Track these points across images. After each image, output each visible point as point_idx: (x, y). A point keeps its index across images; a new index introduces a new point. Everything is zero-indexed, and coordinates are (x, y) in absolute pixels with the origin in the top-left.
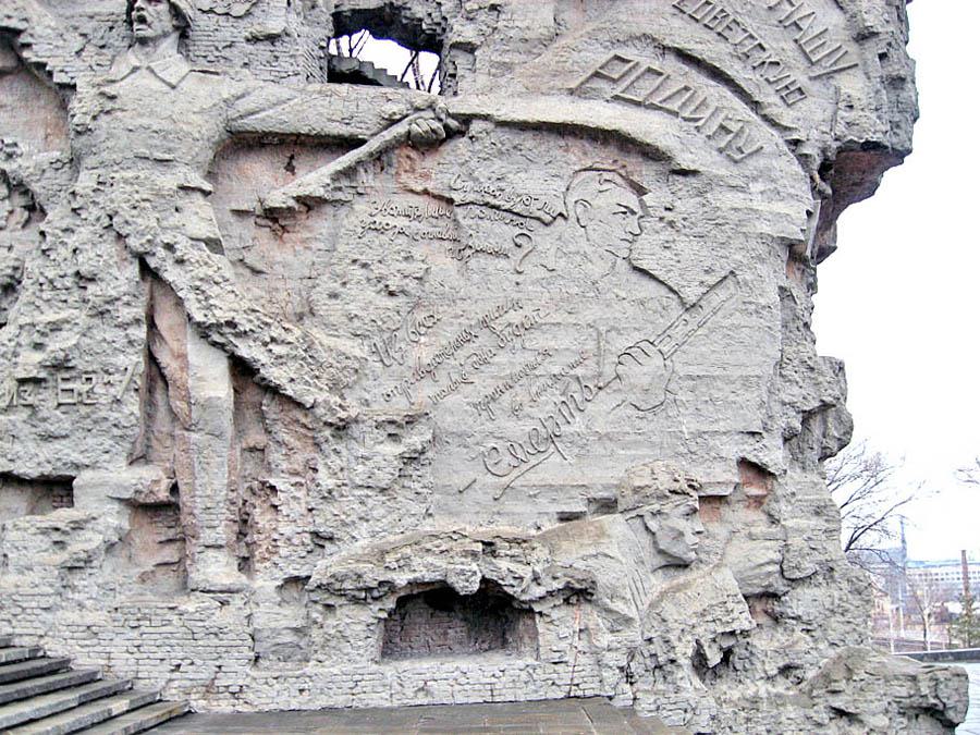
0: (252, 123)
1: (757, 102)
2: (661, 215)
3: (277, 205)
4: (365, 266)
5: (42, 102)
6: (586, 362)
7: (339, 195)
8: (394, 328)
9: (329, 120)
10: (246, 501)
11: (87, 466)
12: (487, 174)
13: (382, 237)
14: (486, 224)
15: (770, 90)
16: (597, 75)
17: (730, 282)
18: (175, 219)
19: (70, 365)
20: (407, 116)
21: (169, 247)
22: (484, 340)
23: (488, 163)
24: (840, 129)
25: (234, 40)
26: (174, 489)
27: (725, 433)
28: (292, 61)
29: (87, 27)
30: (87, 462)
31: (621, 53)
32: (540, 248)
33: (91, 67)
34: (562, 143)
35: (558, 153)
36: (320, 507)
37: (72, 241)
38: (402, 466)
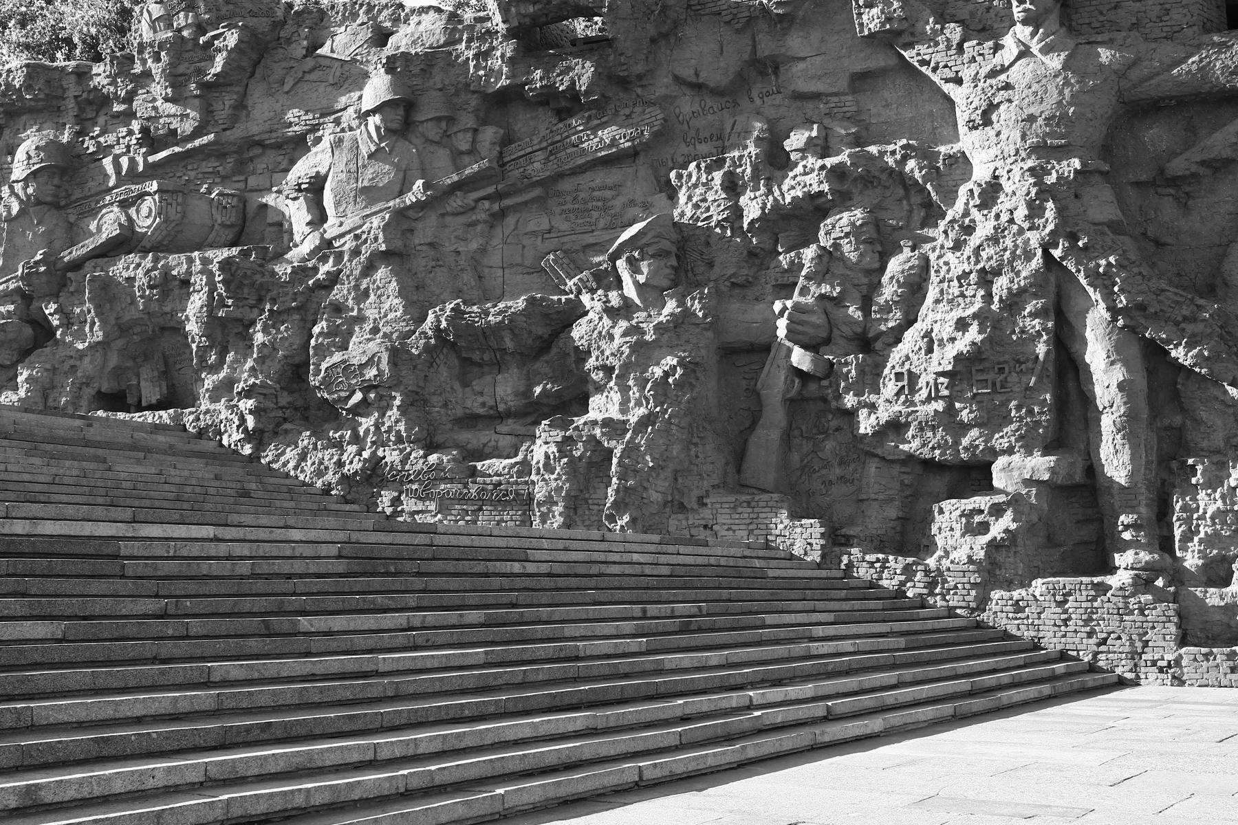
5: (926, 96)
10: (1165, 480)
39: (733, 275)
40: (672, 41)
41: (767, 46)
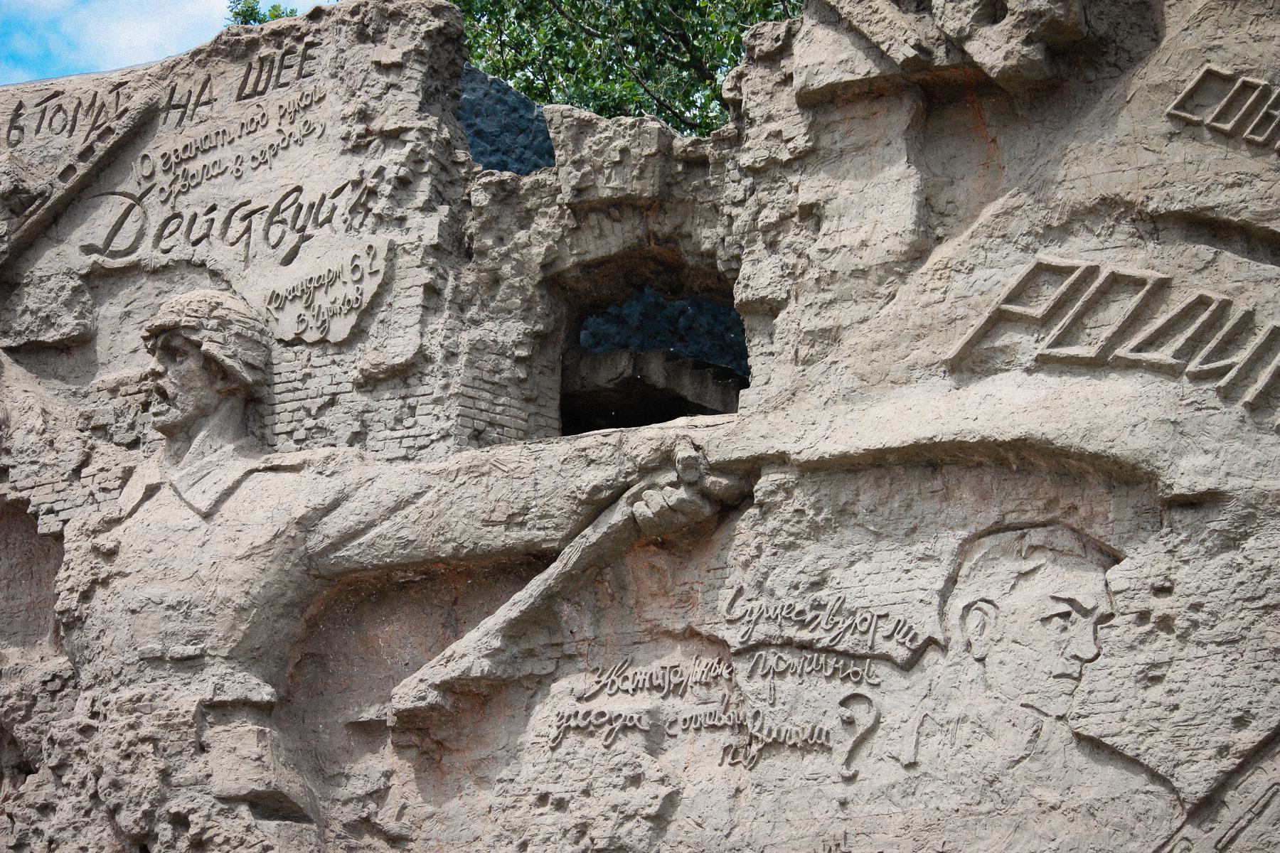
3: (409, 705)
4: (561, 805)
7: (530, 667)
9: (488, 523)
12: (791, 576)
13: (590, 742)
14: (788, 685)
16: (999, 320)
18: (191, 769)
20: (627, 486)
21: (180, 821)
25: (333, 389)
28: (438, 409)
29: (105, 410)
31: (1050, 255)
32: (887, 720)
33: (92, 494)
34: (938, 484)
35: (925, 507)
37: (48, 826)
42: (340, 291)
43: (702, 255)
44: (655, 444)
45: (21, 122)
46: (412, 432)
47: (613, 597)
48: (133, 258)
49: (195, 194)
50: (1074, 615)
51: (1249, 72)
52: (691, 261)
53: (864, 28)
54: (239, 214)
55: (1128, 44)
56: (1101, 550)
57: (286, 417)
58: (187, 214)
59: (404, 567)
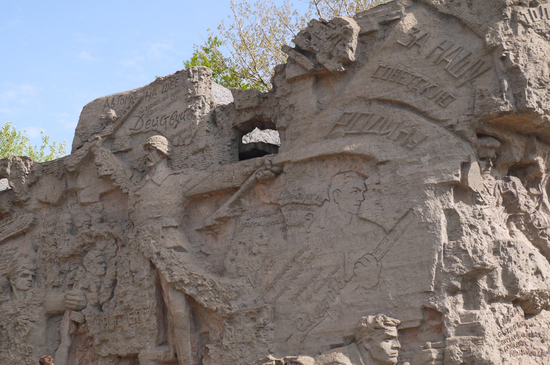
0: (193, 192)
1: (424, 112)
2: (374, 188)
6: (339, 270)
7: (236, 214)
8: (256, 269)
11: (142, 348)
14: (294, 212)
15: (432, 102)
17: (410, 214)
19: (131, 308)
20: (254, 171)
22: (295, 268)
23: (293, 183)
24: (477, 110)
25: (187, 155)
26: (176, 355)
27: (412, 294)
30: (141, 346)
36: (224, 354)
38: (256, 332)
39: (53, 282)
40: (37, 186)
41: (71, 185)
42: (187, 133)
43: (268, 119)
44: (260, 161)
45: (114, 103)
46: (205, 163)
47: (253, 196)
48: (140, 130)
49: (154, 114)
50: (358, 191)
51: (389, 65)
52: (266, 120)
53: (301, 63)
54: (163, 118)
55: (361, 62)
56: (363, 176)
57: (177, 162)
58: (152, 119)
59: (205, 193)
